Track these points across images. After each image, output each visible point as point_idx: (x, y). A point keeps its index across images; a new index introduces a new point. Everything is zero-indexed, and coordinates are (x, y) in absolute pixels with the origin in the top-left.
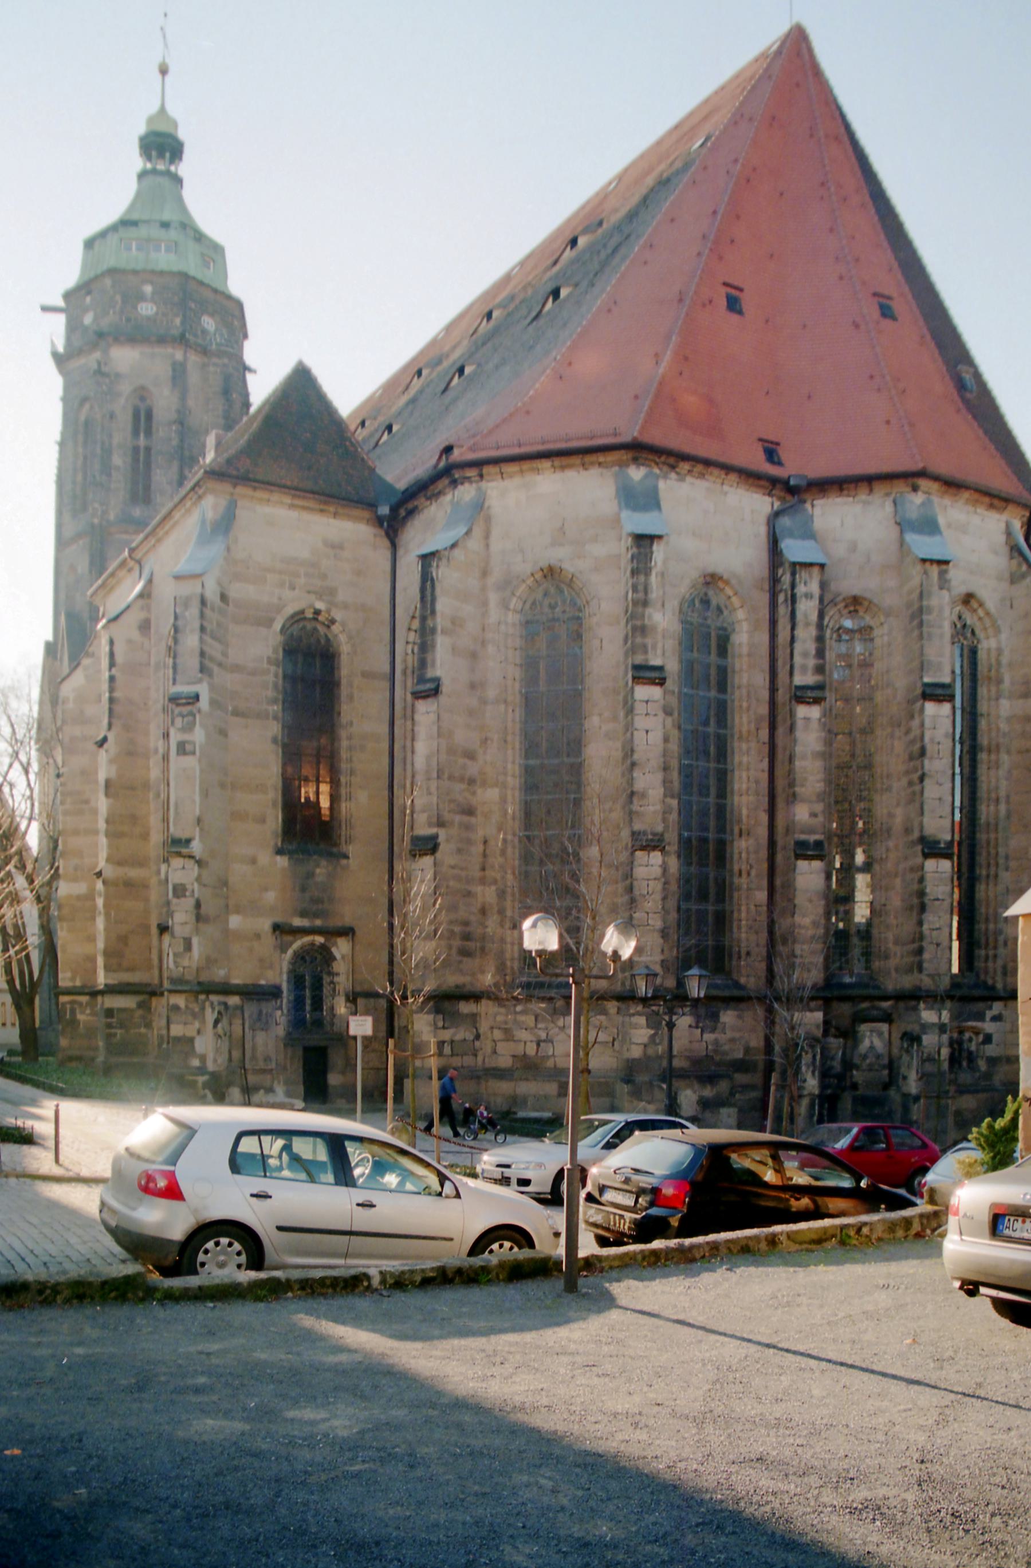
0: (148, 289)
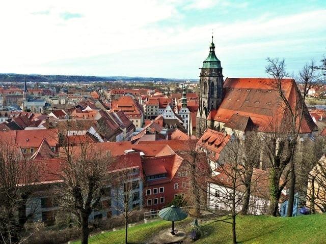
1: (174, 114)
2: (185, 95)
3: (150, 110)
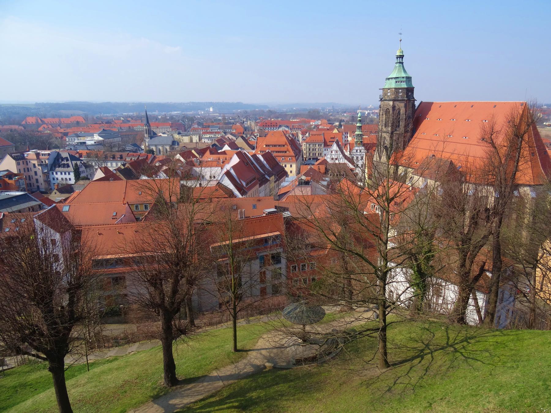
0: (400, 90)
1: (341, 156)
2: (360, 127)
3: (311, 150)
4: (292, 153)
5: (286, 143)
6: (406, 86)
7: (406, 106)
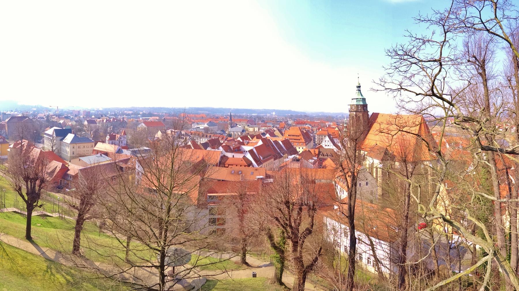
1: (332, 144)
3: (320, 139)
4: (303, 141)
5: (300, 134)
6: (362, 104)
7: (363, 116)
